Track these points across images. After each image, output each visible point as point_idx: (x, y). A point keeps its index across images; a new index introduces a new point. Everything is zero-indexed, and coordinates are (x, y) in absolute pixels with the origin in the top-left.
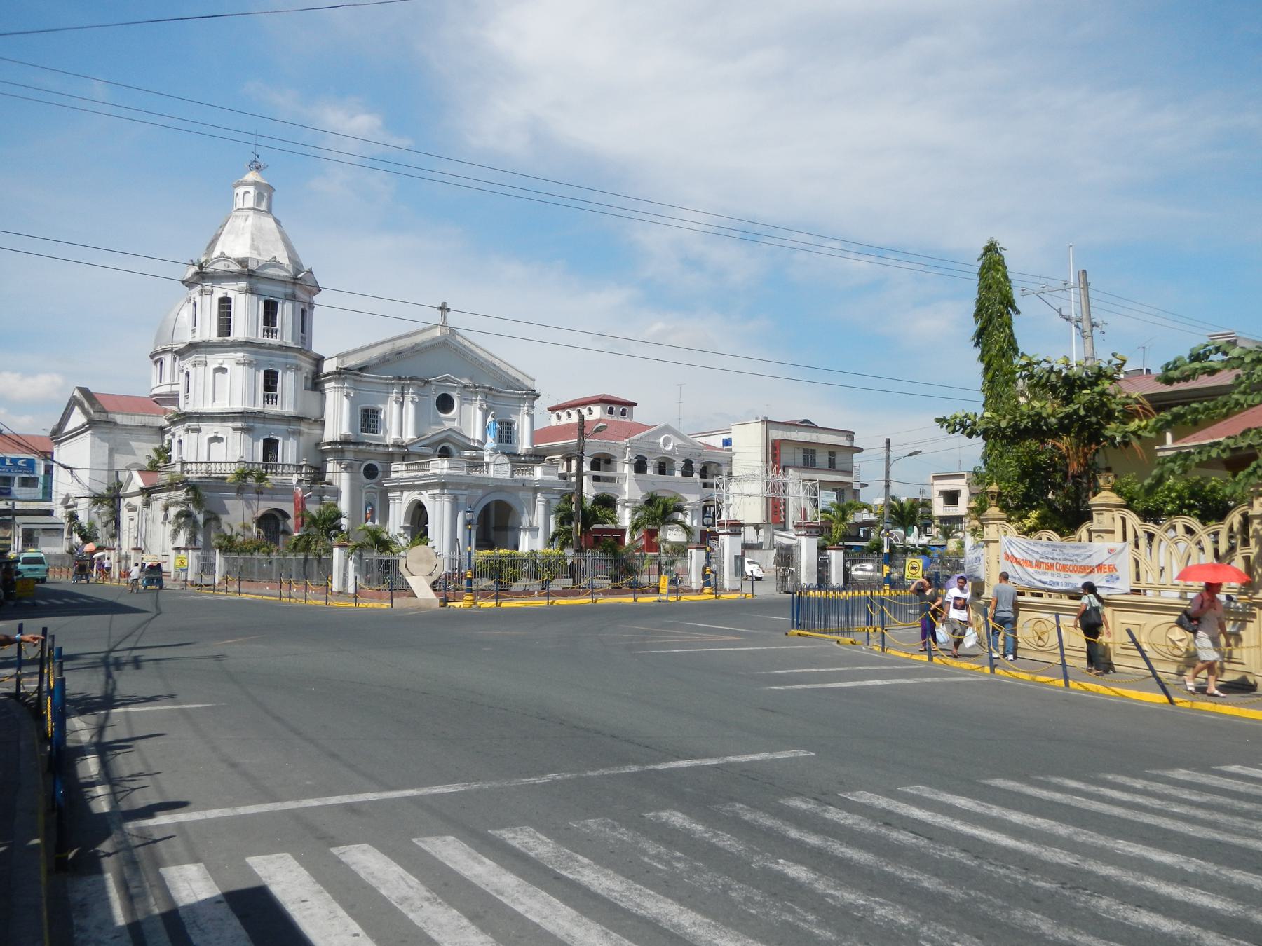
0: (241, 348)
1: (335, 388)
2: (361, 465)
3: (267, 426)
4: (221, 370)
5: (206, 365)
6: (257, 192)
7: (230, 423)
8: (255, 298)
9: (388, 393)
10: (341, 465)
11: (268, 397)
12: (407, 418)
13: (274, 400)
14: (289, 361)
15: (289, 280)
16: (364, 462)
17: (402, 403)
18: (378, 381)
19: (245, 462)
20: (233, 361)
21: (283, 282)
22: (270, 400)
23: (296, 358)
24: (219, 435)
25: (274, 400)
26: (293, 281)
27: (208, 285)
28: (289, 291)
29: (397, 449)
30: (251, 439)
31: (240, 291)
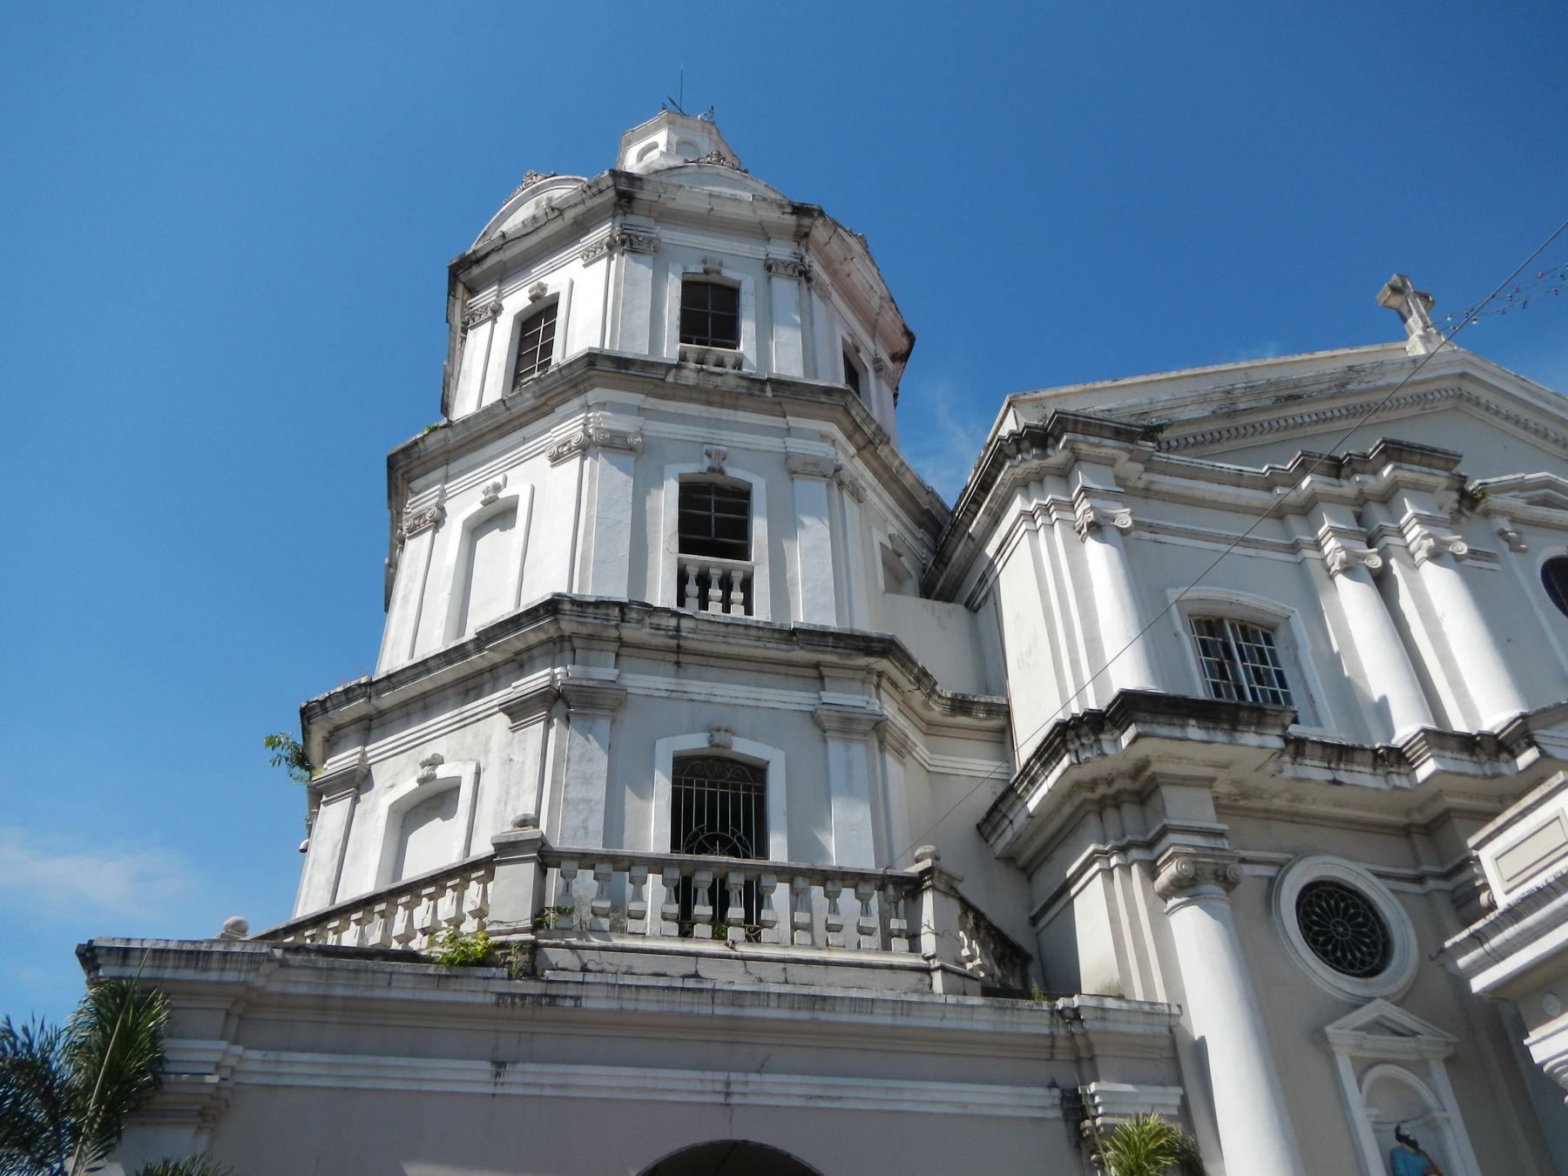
0: (575, 403)
1: (1030, 516)
2: (1272, 887)
3: (697, 687)
4: (498, 515)
5: (438, 522)
6: (675, 139)
7: (500, 696)
8: (644, 272)
9: (1294, 548)
10: (1152, 871)
11: (704, 581)
12: (1437, 637)
13: (737, 595)
14: (796, 445)
15: (772, 215)
16: (1283, 867)
17: (1382, 581)
18: (1228, 493)
19: (545, 857)
20: (543, 460)
21: (763, 232)
22: (715, 592)
23: (823, 437)
24: (442, 772)
25: (737, 595)
26: (791, 220)
27: (487, 297)
28: (782, 251)
29: (1466, 765)
30: (601, 762)
31: (590, 260)
